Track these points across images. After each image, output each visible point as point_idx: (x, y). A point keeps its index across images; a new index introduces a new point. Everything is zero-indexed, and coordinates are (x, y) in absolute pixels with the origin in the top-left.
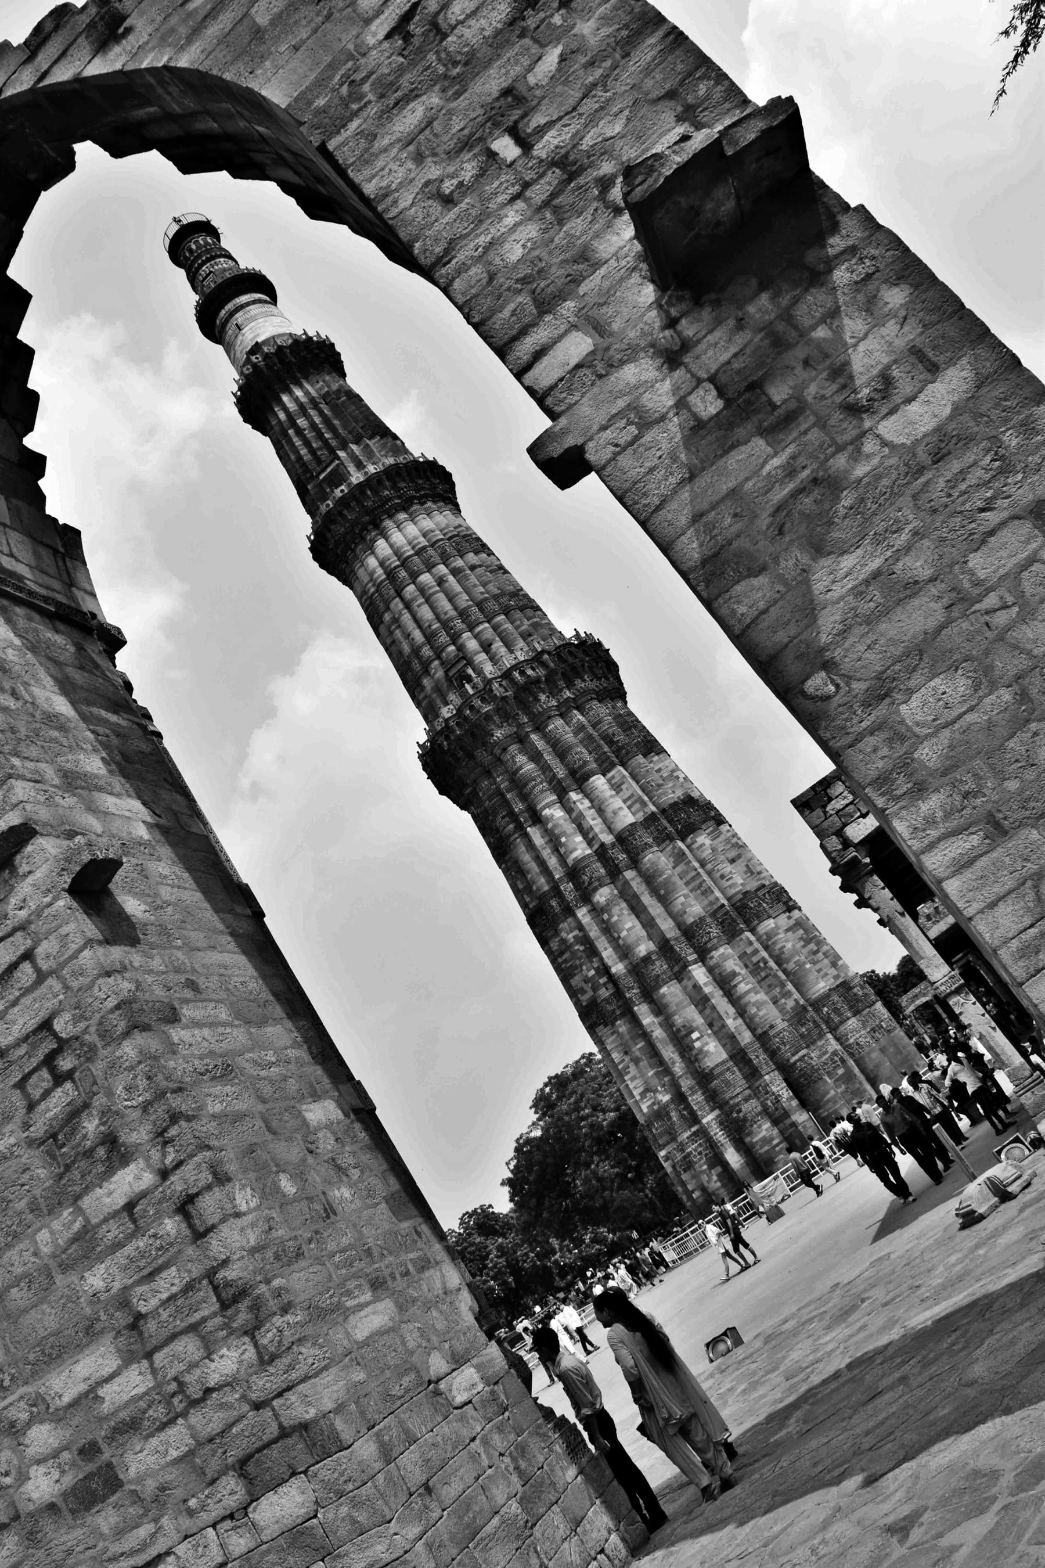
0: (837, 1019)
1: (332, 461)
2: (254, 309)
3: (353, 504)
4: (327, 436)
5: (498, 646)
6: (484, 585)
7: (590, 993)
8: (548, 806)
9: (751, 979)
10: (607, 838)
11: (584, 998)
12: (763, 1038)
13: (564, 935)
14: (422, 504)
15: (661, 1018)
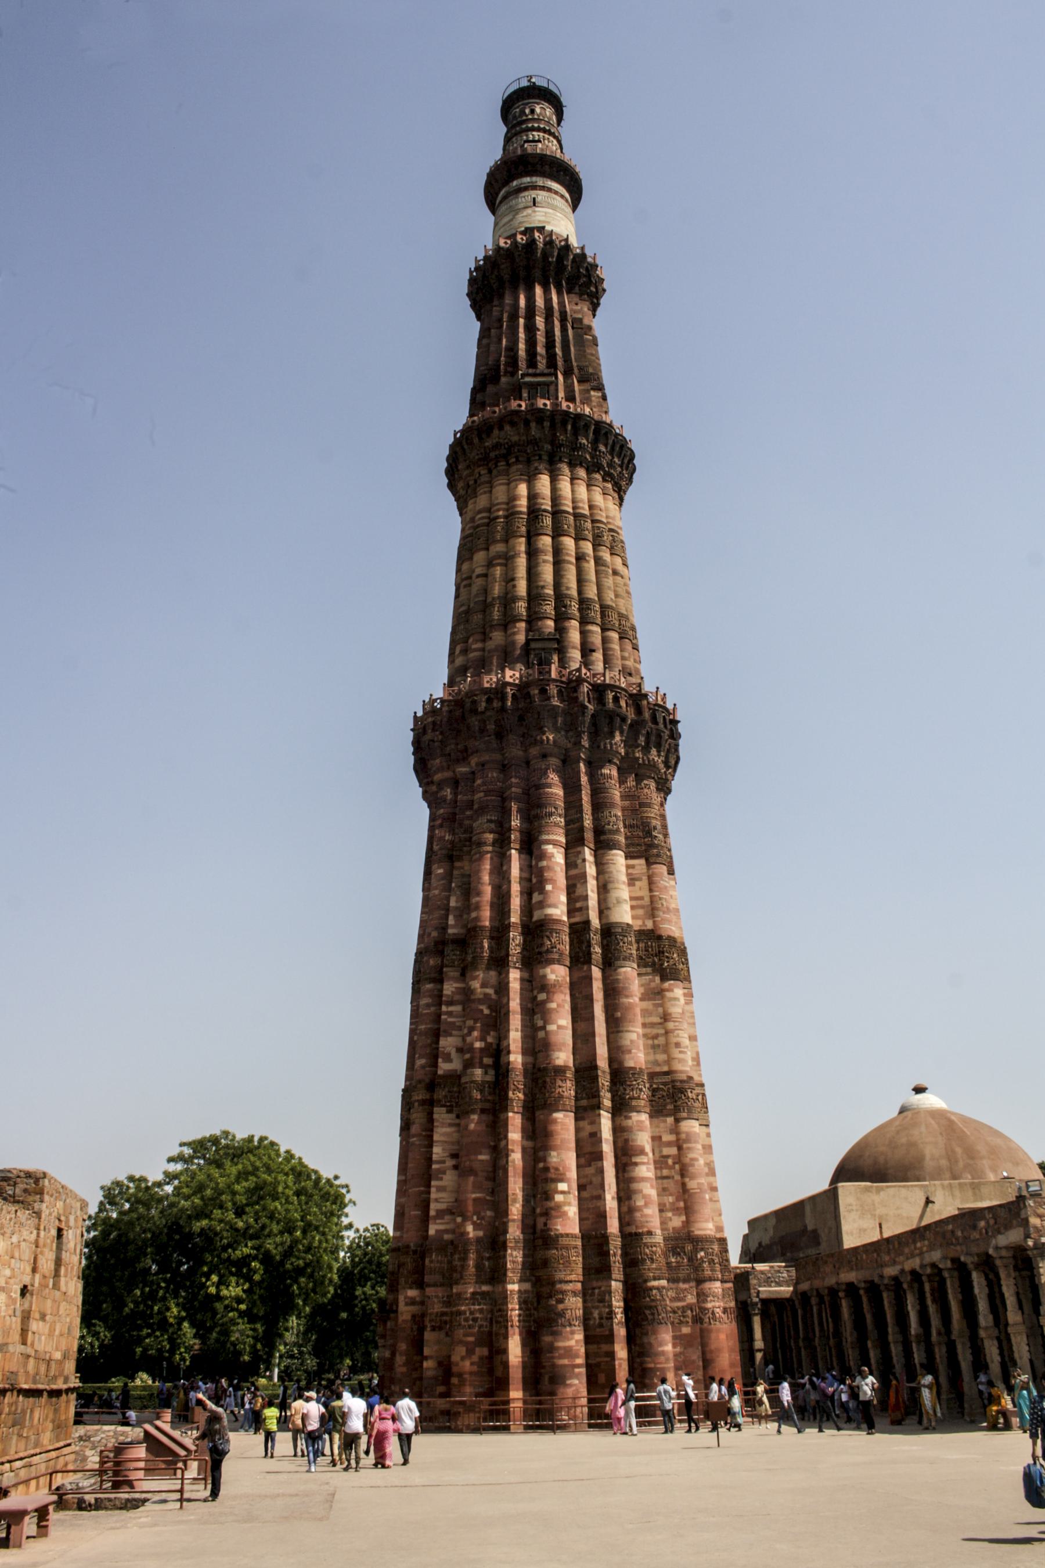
0: (708, 1273)
1: (549, 375)
2: (559, 202)
3: (547, 424)
4: (558, 351)
5: (598, 656)
6: (616, 596)
7: (455, 1065)
8: (555, 843)
9: (652, 1167)
10: (595, 922)
11: (444, 1067)
12: (632, 1238)
13: (476, 985)
14: (604, 480)
15: (529, 1144)
